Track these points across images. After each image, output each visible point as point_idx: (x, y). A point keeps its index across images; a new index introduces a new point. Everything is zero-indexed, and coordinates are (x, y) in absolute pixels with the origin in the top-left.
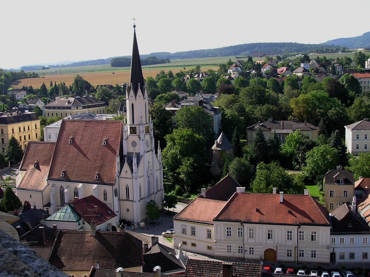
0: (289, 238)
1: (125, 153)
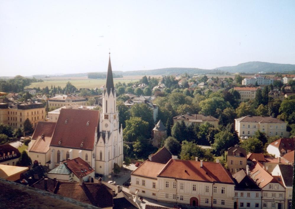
0: (207, 190)
1: (101, 131)
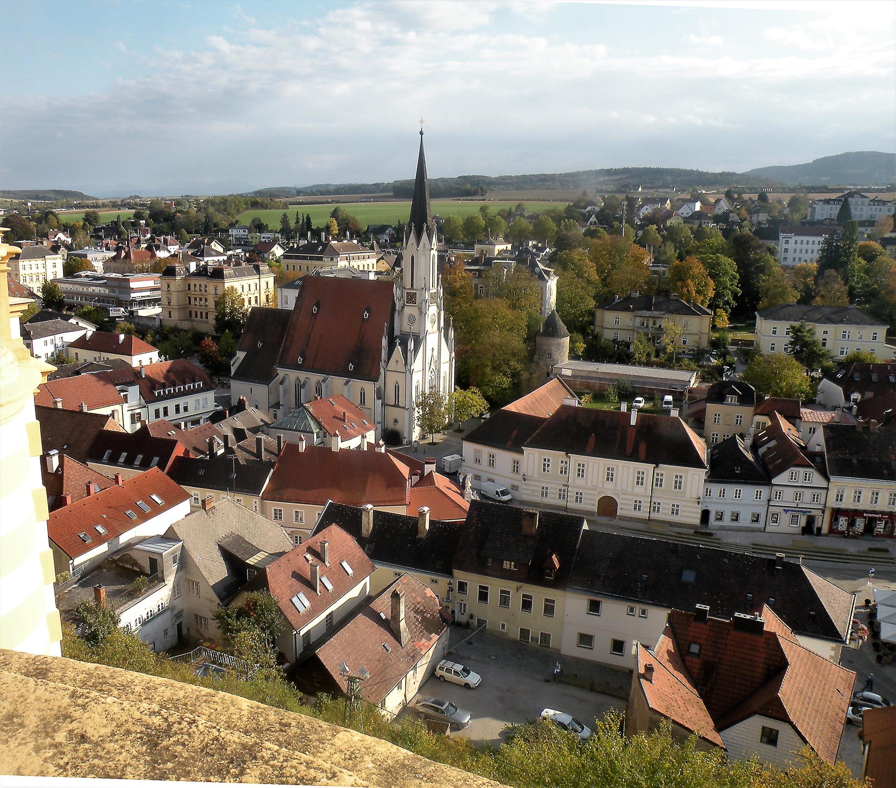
0: (640, 481)
1: (397, 332)
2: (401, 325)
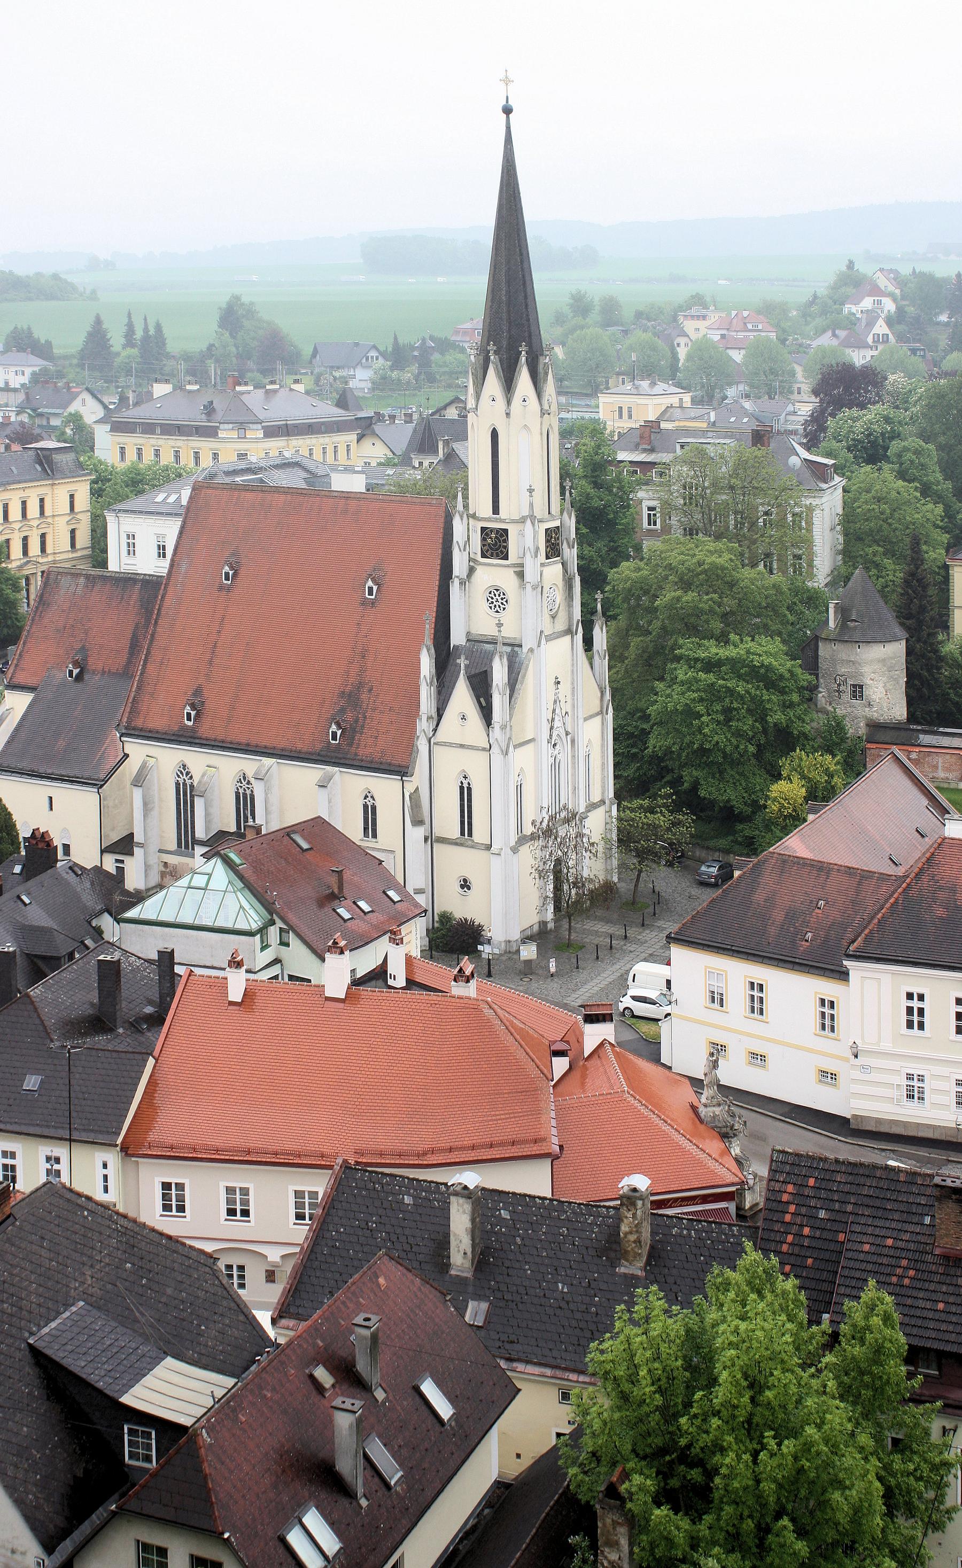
1: (457, 637)
2: (469, 617)
